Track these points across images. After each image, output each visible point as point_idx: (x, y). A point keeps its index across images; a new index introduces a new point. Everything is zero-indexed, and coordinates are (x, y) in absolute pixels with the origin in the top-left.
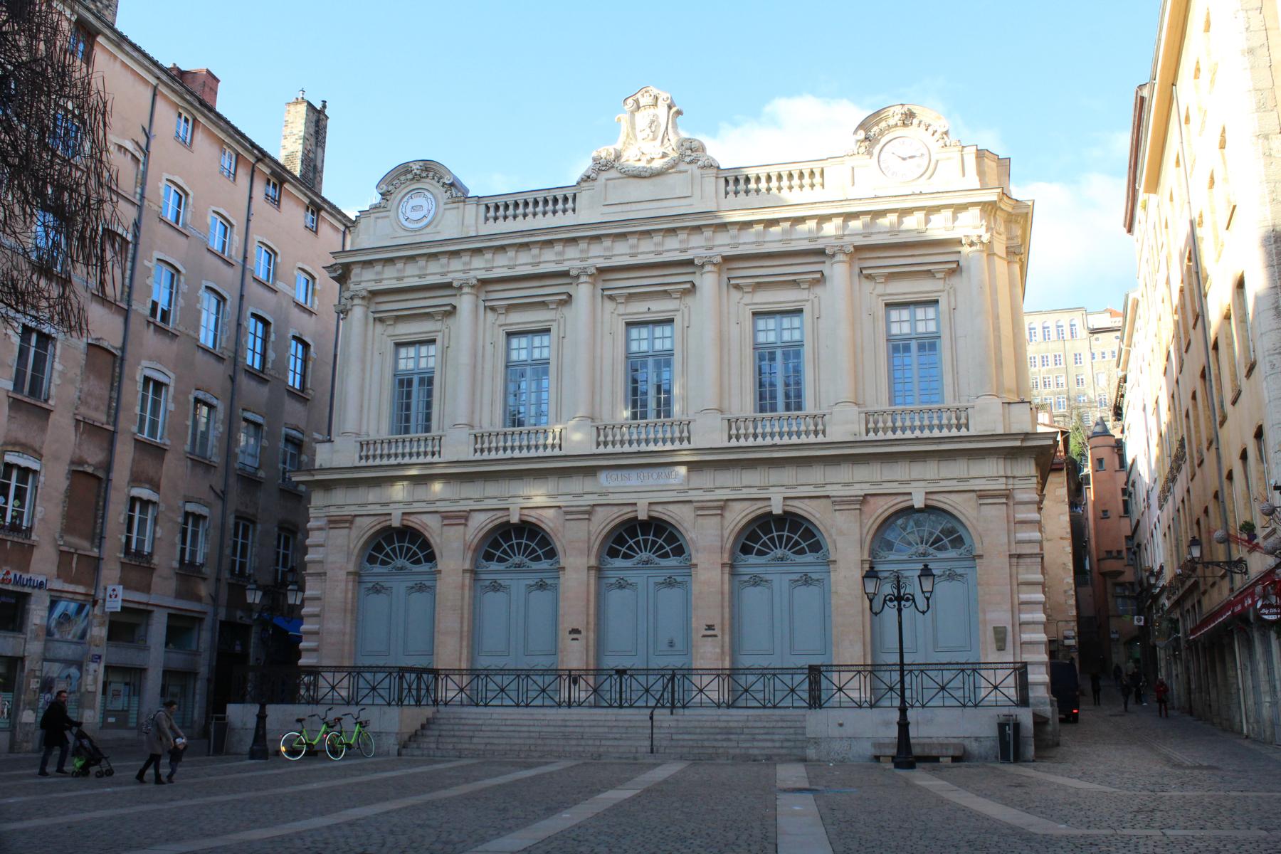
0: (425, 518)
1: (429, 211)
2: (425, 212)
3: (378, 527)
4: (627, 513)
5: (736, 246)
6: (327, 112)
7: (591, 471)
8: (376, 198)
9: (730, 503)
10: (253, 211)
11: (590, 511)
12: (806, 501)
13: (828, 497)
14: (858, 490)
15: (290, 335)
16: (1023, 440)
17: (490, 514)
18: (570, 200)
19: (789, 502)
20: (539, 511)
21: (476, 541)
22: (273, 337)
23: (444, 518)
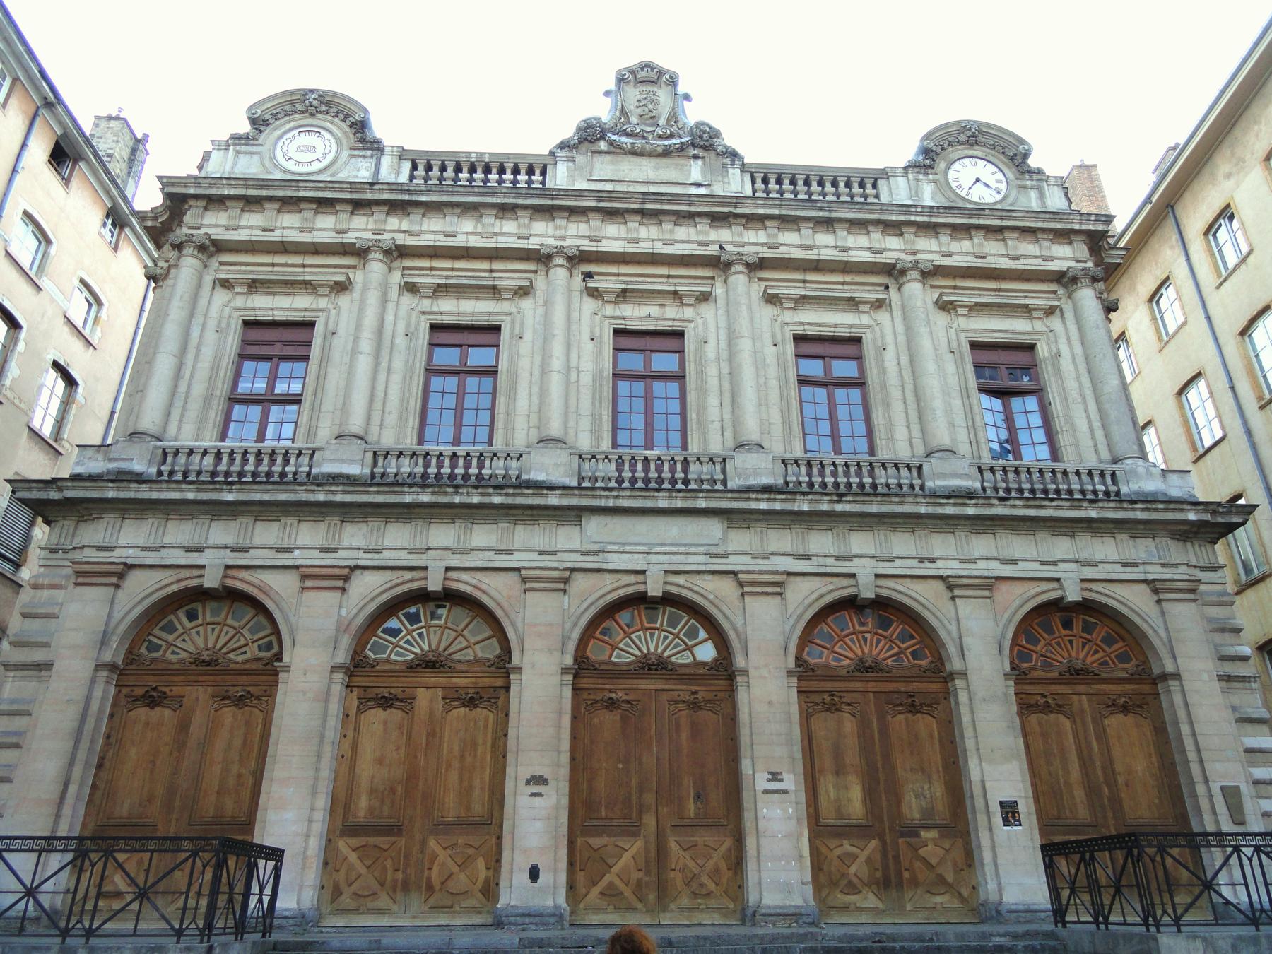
0: (269, 578)
1: (325, 155)
2: (319, 154)
3: (175, 588)
4: (629, 586)
5: (777, 246)
6: (147, 146)
7: (575, 514)
8: (245, 127)
9: (792, 578)
10: (23, 162)
11: (563, 580)
12: (908, 580)
13: (940, 577)
14: (981, 568)
15: (50, 358)
16: (1214, 513)
17: (389, 575)
18: (537, 172)
19: (882, 582)
20: (479, 575)
21: (360, 619)
22: (21, 346)
23: (304, 577)
